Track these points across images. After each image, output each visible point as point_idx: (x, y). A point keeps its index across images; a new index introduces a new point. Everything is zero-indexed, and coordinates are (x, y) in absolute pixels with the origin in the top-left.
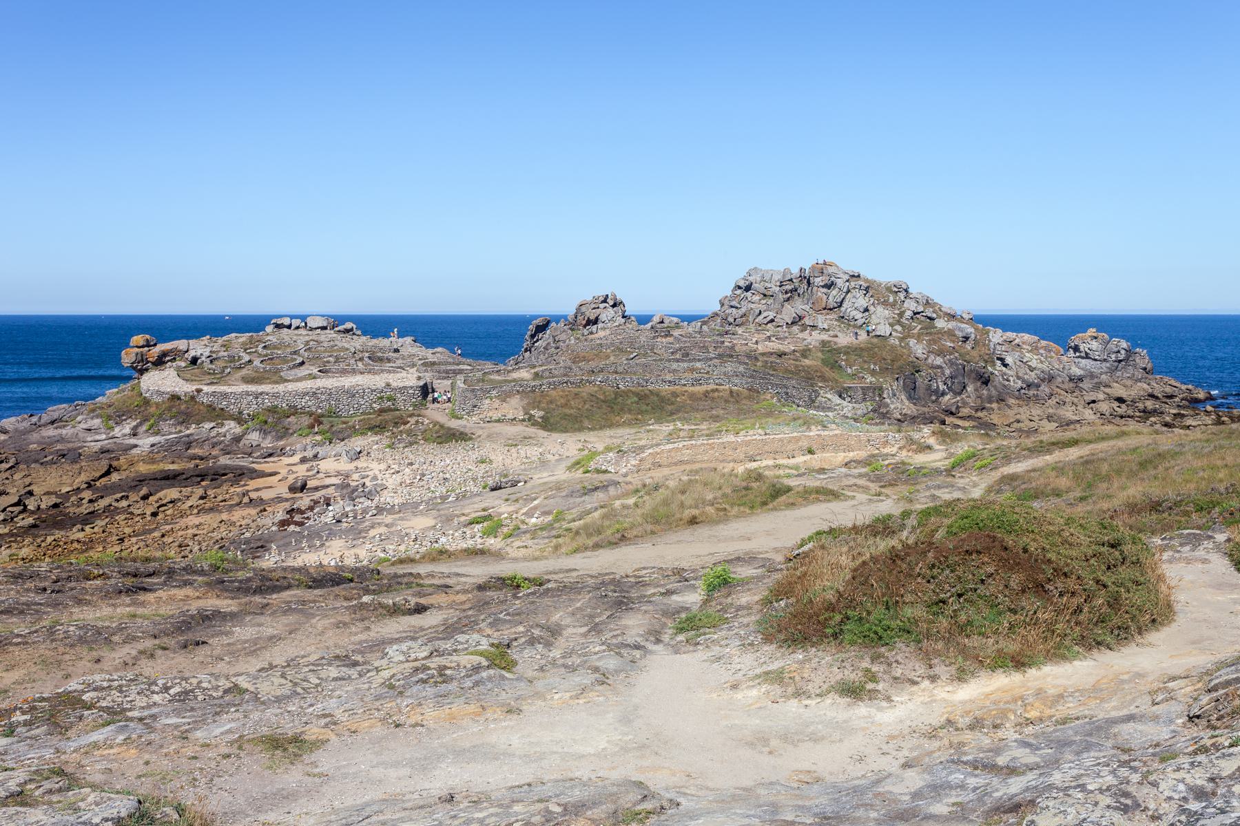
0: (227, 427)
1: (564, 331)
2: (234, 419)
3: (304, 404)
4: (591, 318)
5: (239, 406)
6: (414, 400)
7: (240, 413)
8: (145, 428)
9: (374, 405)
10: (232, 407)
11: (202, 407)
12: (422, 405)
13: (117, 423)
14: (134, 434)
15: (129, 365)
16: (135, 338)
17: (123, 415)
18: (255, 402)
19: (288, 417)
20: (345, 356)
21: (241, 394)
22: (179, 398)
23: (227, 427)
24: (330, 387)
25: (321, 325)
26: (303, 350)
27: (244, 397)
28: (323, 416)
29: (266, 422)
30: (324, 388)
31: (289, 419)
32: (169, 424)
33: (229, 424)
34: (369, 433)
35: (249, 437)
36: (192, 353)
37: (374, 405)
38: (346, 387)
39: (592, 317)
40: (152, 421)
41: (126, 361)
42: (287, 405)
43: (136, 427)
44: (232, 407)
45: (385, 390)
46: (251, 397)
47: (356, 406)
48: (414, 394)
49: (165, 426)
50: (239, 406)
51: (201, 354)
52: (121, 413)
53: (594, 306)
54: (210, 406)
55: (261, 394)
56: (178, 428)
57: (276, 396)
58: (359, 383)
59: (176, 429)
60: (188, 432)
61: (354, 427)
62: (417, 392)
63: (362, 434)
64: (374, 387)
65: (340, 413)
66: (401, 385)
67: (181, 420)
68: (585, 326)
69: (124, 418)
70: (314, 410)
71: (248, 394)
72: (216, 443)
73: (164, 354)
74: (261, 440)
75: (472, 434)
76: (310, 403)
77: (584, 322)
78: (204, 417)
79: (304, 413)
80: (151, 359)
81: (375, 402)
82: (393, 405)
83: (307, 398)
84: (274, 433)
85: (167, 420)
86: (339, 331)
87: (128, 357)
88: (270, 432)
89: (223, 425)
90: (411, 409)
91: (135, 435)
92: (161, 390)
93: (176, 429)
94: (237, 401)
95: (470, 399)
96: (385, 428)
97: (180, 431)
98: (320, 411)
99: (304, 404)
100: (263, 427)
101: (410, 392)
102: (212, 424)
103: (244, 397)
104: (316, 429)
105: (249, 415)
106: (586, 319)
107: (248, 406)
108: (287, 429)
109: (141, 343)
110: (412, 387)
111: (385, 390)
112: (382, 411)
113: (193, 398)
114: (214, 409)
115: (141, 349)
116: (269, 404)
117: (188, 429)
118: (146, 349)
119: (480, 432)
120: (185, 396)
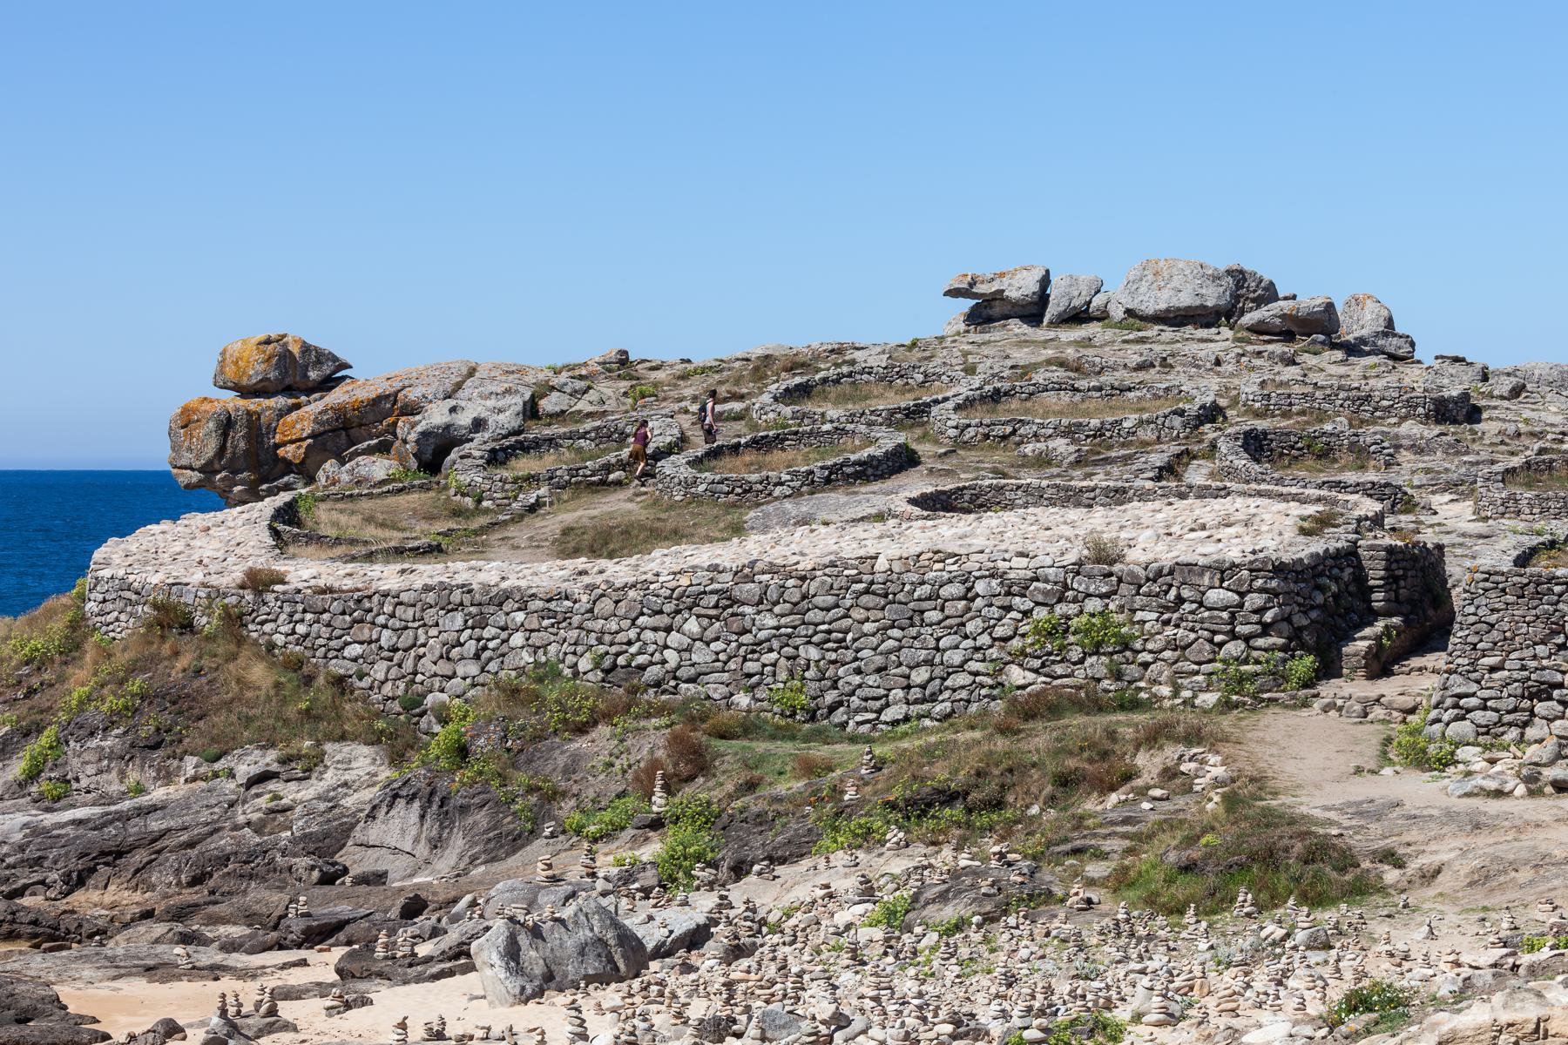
0: (330, 778)
2: (374, 739)
5: (409, 665)
6: (1234, 648)
7: (413, 704)
9: (1016, 675)
11: (259, 673)
12: (1279, 678)
15: (195, 476)
18: (471, 647)
19: (582, 730)
20: (1147, 434)
22: (187, 626)
23: (330, 778)
24: (806, 565)
25: (1185, 300)
26: (950, 405)
27: (430, 616)
28: (748, 728)
29: (462, 752)
30: (773, 569)
31: (581, 744)
32: (101, 754)
33: (347, 763)
34: (895, 835)
35: (374, 833)
36: (436, 416)
37: (1016, 675)
38: (881, 564)
40: (46, 738)
42: (597, 666)
44: (379, 670)
45: (1080, 584)
46: (459, 619)
47: (920, 675)
48: (1234, 610)
49: (82, 762)
50: (409, 665)
51: (479, 424)
54: (296, 664)
55: (501, 599)
56: (133, 776)
59: (122, 775)
60: (158, 794)
61: (837, 791)
62: (1254, 600)
63: (867, 838)
64: (1019, 569)
65: (839, 716)
66: (1167, 555)
67: (146, 731)
70: (717, 692)
72: (225, 859)
74: (422, 850)
75: (1391, 857)
76: (701, 655)
78: (249, 720)
79: (660, 711)
80: (288, 452)
81: (1020, 657)
82: (1118, 676)
83: (693, 626)
84: (481, 818)
86: (1259, 329)
88: (464, 810)
89: (313, 764)
90: (1209, 699)
92: (136, 580)
93: (122, 775)
94: (403, 642)
95: (1507, 643)
96: (998, 804)
97: (140, 790)
98: (743, 700)
99: (672, 657)
100: (443, 784)
101: (1214, 596)
102: (269, 759)
103: (430, 616)
104: (659, 802)
107: (444, 668)
108: (555, 795)
110: (1224, 571)
111: (1080, 584)
112: (1033, 709)
113: (235, 621)
114: (309, 680)
115: (253, 404)
116: (527, 657)
117: (167, 777)
118: (280, 401)
119: (1441, 852)
120: (208, 610)
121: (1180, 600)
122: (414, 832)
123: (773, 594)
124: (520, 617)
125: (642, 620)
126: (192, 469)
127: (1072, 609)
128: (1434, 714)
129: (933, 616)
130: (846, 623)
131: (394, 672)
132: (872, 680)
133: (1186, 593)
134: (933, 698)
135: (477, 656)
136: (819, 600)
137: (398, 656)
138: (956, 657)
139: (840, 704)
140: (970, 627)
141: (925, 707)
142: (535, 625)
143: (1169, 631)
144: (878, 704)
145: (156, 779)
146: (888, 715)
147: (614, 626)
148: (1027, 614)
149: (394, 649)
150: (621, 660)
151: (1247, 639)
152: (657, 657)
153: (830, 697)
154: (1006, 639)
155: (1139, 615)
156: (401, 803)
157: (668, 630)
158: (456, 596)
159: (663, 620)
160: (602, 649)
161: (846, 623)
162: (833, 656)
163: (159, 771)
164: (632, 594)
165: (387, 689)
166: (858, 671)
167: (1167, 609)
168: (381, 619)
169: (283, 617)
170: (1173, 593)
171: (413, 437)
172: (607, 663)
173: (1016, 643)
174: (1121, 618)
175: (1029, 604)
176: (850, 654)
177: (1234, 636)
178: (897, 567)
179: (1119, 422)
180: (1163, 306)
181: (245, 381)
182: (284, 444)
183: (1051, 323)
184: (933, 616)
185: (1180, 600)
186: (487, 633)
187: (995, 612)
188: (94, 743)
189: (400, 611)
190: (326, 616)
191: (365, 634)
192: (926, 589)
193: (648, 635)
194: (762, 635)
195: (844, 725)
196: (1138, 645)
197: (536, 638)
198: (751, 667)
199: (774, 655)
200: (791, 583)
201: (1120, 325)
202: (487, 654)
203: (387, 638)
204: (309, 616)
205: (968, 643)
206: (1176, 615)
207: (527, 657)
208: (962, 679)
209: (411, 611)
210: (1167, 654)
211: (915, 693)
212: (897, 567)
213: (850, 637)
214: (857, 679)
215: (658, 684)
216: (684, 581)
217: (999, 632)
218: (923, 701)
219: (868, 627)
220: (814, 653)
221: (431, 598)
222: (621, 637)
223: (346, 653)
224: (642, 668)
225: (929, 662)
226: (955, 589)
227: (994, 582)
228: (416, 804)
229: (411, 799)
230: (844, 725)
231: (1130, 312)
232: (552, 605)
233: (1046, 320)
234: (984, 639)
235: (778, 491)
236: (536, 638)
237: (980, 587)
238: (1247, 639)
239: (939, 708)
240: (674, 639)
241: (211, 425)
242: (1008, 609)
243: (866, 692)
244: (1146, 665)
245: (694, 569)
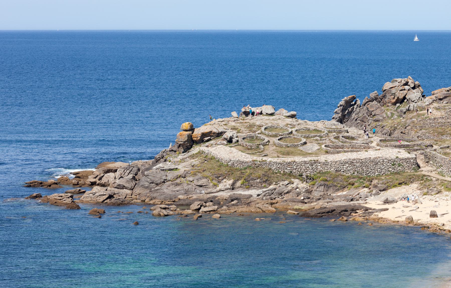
1: (378, 108)
3: (345, 169)
4: (400, 98)
6: (414, 166)
8: (239, 184)
9: (390, 169)
10: (294, 171)
13: (219, 182)
14: (233, 188)
16: (184, 124)
17: (220, 177)
18: (311, 168)
21: (301, 163)
24: (361, 158)
32: (257, 182)
38: (372, 158)
39: (401, 97)
41: (181, 140)
43: (233, 184)
45: (396, 160)
46: (308, 165)
47: (379, 170)
52: (219, 175)
53: (401, 88)
57: (326, 163)
58: (380, 156)
59: (262, 185)
64: (390, 159)
65: (369, 174)
68: (395, 104)
69: (220, 178)
71: (305, 162)
73: (204, 135)
76: (349, 168)
77: (394, 100)
80: (195, 139)
83: (347, 165)
85: (255, 180)
87: (183, 136)
91: (233, 189)
101: (412, 161)
102: (286, 182)
103: (302, 164)
105: (307, 176)
106: (396, 98)
109: (188, 128)
110: (412, 158)
116: (321, 169)
117: (270, 185)
121: (408, 161)
122: (323, 189)
123: (358, 161)
124: (319, 164)
125: (340, 165)
126: (182, 142)
127: (396, 162)
128: (448, 172)
129: (380, 164)
130: (368, 164)
131: (297, 171)
132: (373, 170)
133: (409, 161)
134: (381, 172)
135: (312, 169)
136: (365, 162)
137: (297, 169)
138: (383, 168)
139: (369, 173)
140: (384, 165)
141: (380, 173)
142: (322, 165)
143: (407, 165)
144: (374, 173)
145: (268, 185)
146: (376, 174)
147: (336, 165)
148: (391, 163)
149: (296, 168)
150: (338, 169)
151: (415, 165)
152: (343, 169)
153: (368, 172)
154: (388, 166)
155: (403, 163)
156: (321, 186)
157: (344, 166)
158: (307, 162)
159: (343, 165)
160: (335, 168)
161: (368, 164)
162: (367, 168)
163: (268, 184)
164: (338, 162)
165: (296, 173)
166: (371, 170)
167: (406, 162)
168: (294, 165)
169: (275, 165)
170: (407, 161)
171: (229, 138)
172: (336, 169)
173: (390, 166)
174: (401, 163)
175: (391, 162)
176: (370, 168)
177: (413, 165)
178: (374, 158)
179: (321, 135)
180: (271, 113)
181: (187, 129)
182: (194, 138)
183: (256, 115)
184: (380, 164)
185: (408, 161)
186: (313, 166)
187: (387, 163)
188: (256, 181)
189: (296, 164)
190: (283, 165)
191: (291, 167)
192: (378, 161)
193: (342, 166)
194: (357, 166)
195: (370, 175)
196: (404, 166)
197: (322, 167)
198: (356, 169)
199: (359, 168)
200: (360, 160)
201: (265, 115)
202: (313, 169)
203: (295, 167)
204: (280, 165)
205: (384, 166)
206: (407, 163)
207: (321, 169)
208: (384, 170)
209: (299, 164)
210: (407, 167)
211: (379, 172)
212: (374, 158)
213: (369, 166)
214: (371, 171)
215: (343, 172)
216: (346, 160)
217: (388, 165)
218: (379, 172)
219: (371, 165)
220: (365, 168)
221: (302, 162)
222: (337, 167)
223: (288, 169)
224: (341, 170)
225: (380, 168)
226: (382, 161)
227: (387, 160)
228: (323, 186)
229: (322, 186)
230: (370, 175)
231: (267, 114)
232: (325, 163)
233: (255, 115)
234: (386, 166)
235: (299, 146)
236: (322, 167)
237: (385, 160)
238: (415, 165)
239: (382, 173)
240: (344, 167)
241: (187, 136)
242: (388, 163)
243: (373, 172)
244: (405, 168)
245: (347, 159)
